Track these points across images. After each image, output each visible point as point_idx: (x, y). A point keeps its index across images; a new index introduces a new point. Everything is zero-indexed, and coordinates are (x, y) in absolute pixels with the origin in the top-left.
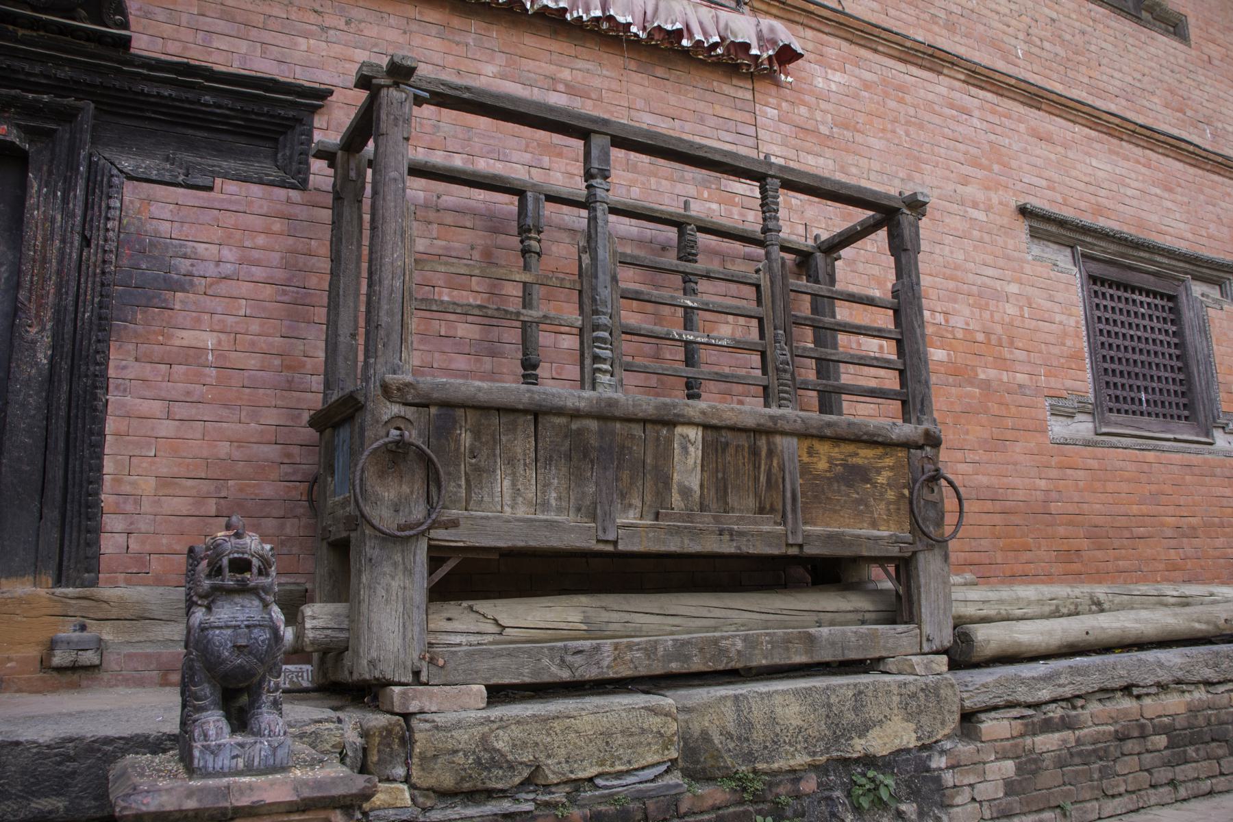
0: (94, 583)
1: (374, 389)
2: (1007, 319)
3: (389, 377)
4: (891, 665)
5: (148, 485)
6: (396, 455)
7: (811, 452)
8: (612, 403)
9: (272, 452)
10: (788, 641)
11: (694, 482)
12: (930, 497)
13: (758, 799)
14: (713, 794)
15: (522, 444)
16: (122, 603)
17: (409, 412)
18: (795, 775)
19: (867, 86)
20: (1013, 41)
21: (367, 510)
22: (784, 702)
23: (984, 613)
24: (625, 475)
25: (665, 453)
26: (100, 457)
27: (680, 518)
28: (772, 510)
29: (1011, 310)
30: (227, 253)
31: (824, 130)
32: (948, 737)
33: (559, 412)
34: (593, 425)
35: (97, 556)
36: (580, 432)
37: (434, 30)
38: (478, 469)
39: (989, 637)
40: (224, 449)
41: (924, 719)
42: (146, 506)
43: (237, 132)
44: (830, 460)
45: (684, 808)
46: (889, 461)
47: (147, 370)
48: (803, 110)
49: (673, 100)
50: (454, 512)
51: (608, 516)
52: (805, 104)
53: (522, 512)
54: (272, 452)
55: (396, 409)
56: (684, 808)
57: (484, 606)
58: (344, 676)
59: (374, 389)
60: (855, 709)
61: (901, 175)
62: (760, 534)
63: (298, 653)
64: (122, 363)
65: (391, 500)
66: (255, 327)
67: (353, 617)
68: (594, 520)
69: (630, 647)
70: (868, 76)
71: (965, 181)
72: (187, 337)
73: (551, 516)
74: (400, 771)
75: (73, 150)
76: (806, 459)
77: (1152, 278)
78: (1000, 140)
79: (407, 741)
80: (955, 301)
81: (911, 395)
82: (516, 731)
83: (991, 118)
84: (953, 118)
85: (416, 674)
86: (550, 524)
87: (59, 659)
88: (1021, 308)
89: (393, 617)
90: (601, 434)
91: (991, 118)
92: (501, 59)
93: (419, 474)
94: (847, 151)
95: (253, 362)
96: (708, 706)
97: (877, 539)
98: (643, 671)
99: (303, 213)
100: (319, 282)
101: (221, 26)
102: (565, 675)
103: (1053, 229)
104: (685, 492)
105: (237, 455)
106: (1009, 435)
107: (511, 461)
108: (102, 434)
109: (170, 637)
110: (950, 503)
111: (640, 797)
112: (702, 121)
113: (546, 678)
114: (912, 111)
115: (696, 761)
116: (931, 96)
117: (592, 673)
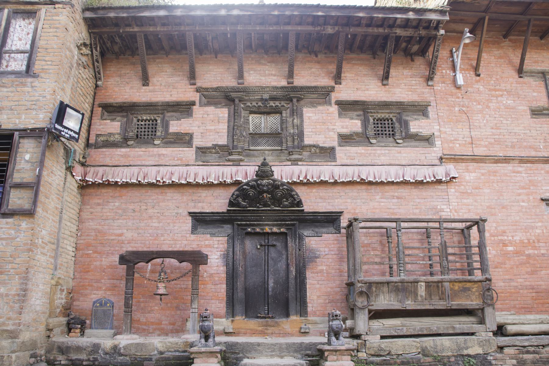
0: (307, 317)
1: (356, 281)
2: (537, 234)
3: (359, 279)
4: (477, 334)
5: (315, 297)
6: (361, 293)
7: (453, 285)
8: (403, 279)
9: (338, 289)
10: (448, 328)
11: (423, 294)
12: (488, 294)
13: (439, 361)
14: (429, 359)
15: (385, 289)
16: (312, 320)
17: (363, 285)
18: (449, 357)
19: (483, 174)
20: (538, 144)
21: (356, 304)
22: (446, 341)
23: (514, 322)
24: (408, 294)
25: (416, 288)
26: (306, 292)
27: (420, 302)
28: (443, 299)
29: (538, 231)
30: (326, 249)
31: (469, 191)
32: (493, 352)
33: (393, 282)
34: (400, 284)
35: (307, 312)
36: (397, 286)
37: (364, 191)
38: (377, 295)
39: (511, 329)
40: (329, 289)
41: (485, 347)
42: (315, 302)
43: (325, 222)
44: (459, 287)
45: (422, 361)
46: (476, 286)
47: (313, 275)
48: (462, 187)
49: (424, 194)
50: (373, 303)
51: (404, 302)
52: (463, 185)
53: (386, 302)
54: (338, 289)
55: (360, 285)
56: (422, 361)
57: (380, 320)
58: (354, 334)
59: (356, 281)
60: (464, 344)
61: (496, 198)
62: (440, 304)
63: (346, 330)
64: (309, 274)
65: (361, 302)
66: (333, 264)
67: (355, 323)
68: (401, 303)
69: (410, 329)
70: (483, 171)
71: (519, 195)
72: (320, 268)
73: (392, 303)
74: (364, 350)
75: (295, 232)
76: (452, 287)
78: (533, 178)
79: (365, 345)
80: (516, 232)
81: (484, 269)
82: (386, 344)
83: (529, 172)
84: (514, 176)
85: (367, 333)
86: (392, 304)
87: (302, 331)
88: (543, 230)
89: (362, 323)
90: (402, 286)
91: (529, 172)
92: (380, 194)
93: (366, 296)
94: (477, 195)
95: (333, 271)
96: (427, 341)
97: (472, 304)
98: (413, 334)
99: (340, 238)
100: (345, 253)
101: (320, 200)
102: (396, 334)
104: (421, 296)
105: (331, 290)
106: (538, 269)
107: (383, 293)
108: (306, 288)
109: (324, 327)
110: (495, 295)
111: (412, 359)
112: (433, 198)
113: (392, 334)
114: (499, 178)
115: (424, 352)
116: (506, 171)
117: (401, 334)
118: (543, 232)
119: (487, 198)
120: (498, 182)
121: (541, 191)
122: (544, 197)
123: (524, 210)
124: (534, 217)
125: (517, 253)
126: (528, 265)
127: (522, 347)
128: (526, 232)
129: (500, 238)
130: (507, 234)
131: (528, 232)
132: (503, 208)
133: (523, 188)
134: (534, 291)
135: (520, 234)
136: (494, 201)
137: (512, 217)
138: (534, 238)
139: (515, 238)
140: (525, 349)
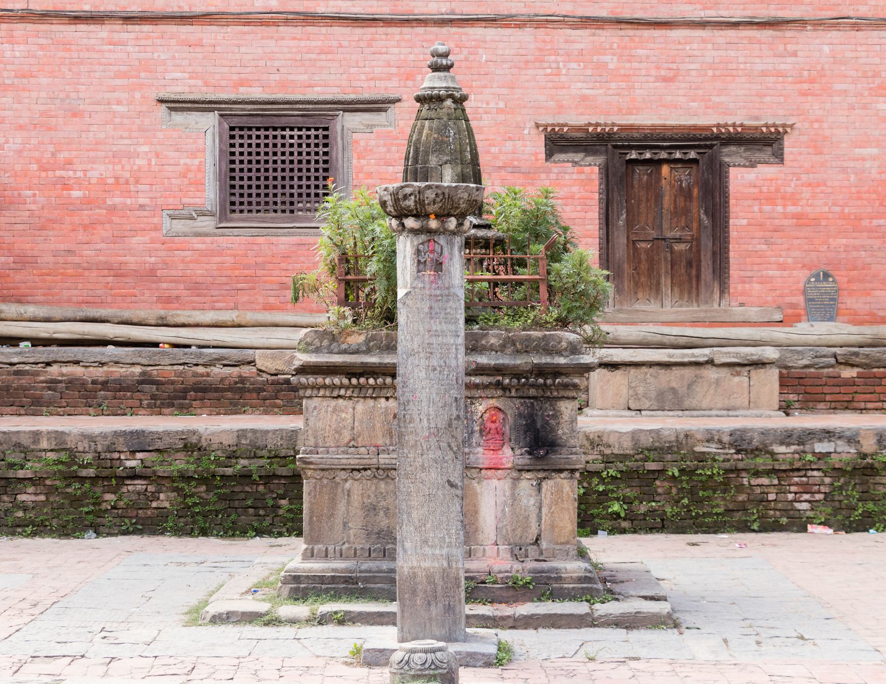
2: (135, 167)
19: (42, 47)
29: (139, 162)
31: (7, 81)
77: (300, 119)
80: (94, 163)
83: (143, 42)
84: (110, 51)
88: (150, 160)
91: (143, 42)
94: (24, 90)
103: (189, 105)
106: (126, 234)
116: (92, 41)
118: (149, 164)
119: (43, 94)
120: (72, 64)
121: (163, 82)
122: (163, 95)
123: (117, 120)
124: (135, 134)
125: (88, 202)
126: (107, 226)
127: (6, 364)
128: (114, 163)
129: (58, 173)
130: (75, 168)
131: (120, 162)
132: (75, 115)
133: (119, 75)
134: (112, 272)
135: (102, 168)
136: (57, 101)
137: (91, 134)
138: (128, 175)
139: (89, 174)
140: (15, 368)
